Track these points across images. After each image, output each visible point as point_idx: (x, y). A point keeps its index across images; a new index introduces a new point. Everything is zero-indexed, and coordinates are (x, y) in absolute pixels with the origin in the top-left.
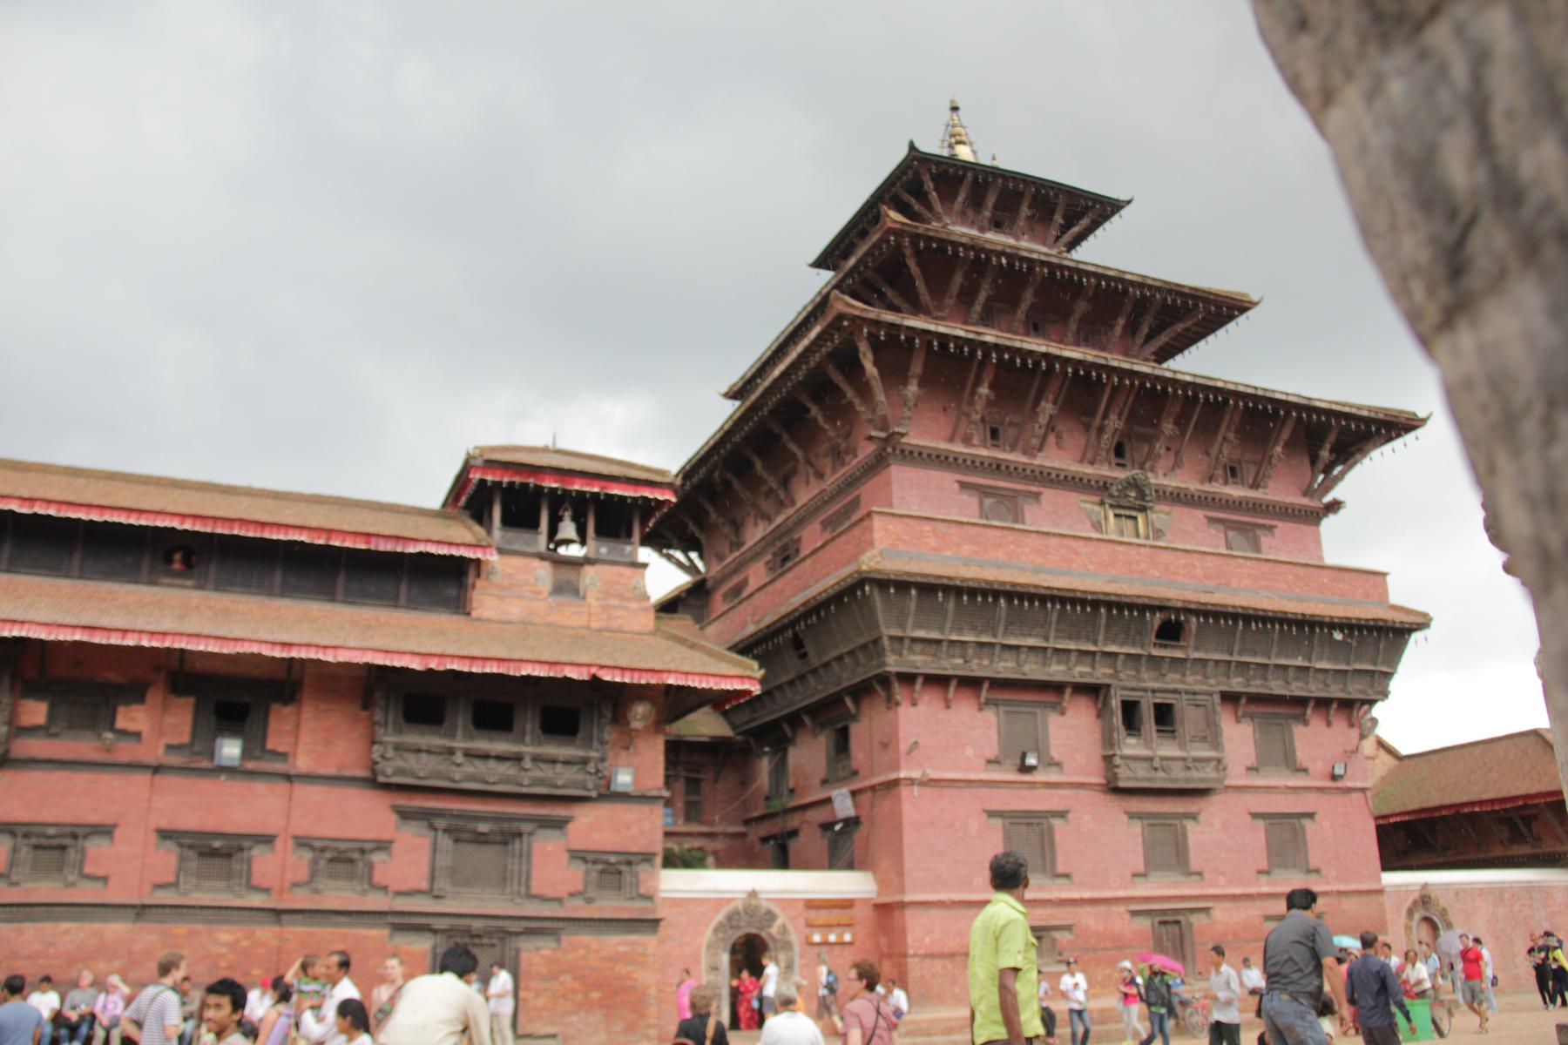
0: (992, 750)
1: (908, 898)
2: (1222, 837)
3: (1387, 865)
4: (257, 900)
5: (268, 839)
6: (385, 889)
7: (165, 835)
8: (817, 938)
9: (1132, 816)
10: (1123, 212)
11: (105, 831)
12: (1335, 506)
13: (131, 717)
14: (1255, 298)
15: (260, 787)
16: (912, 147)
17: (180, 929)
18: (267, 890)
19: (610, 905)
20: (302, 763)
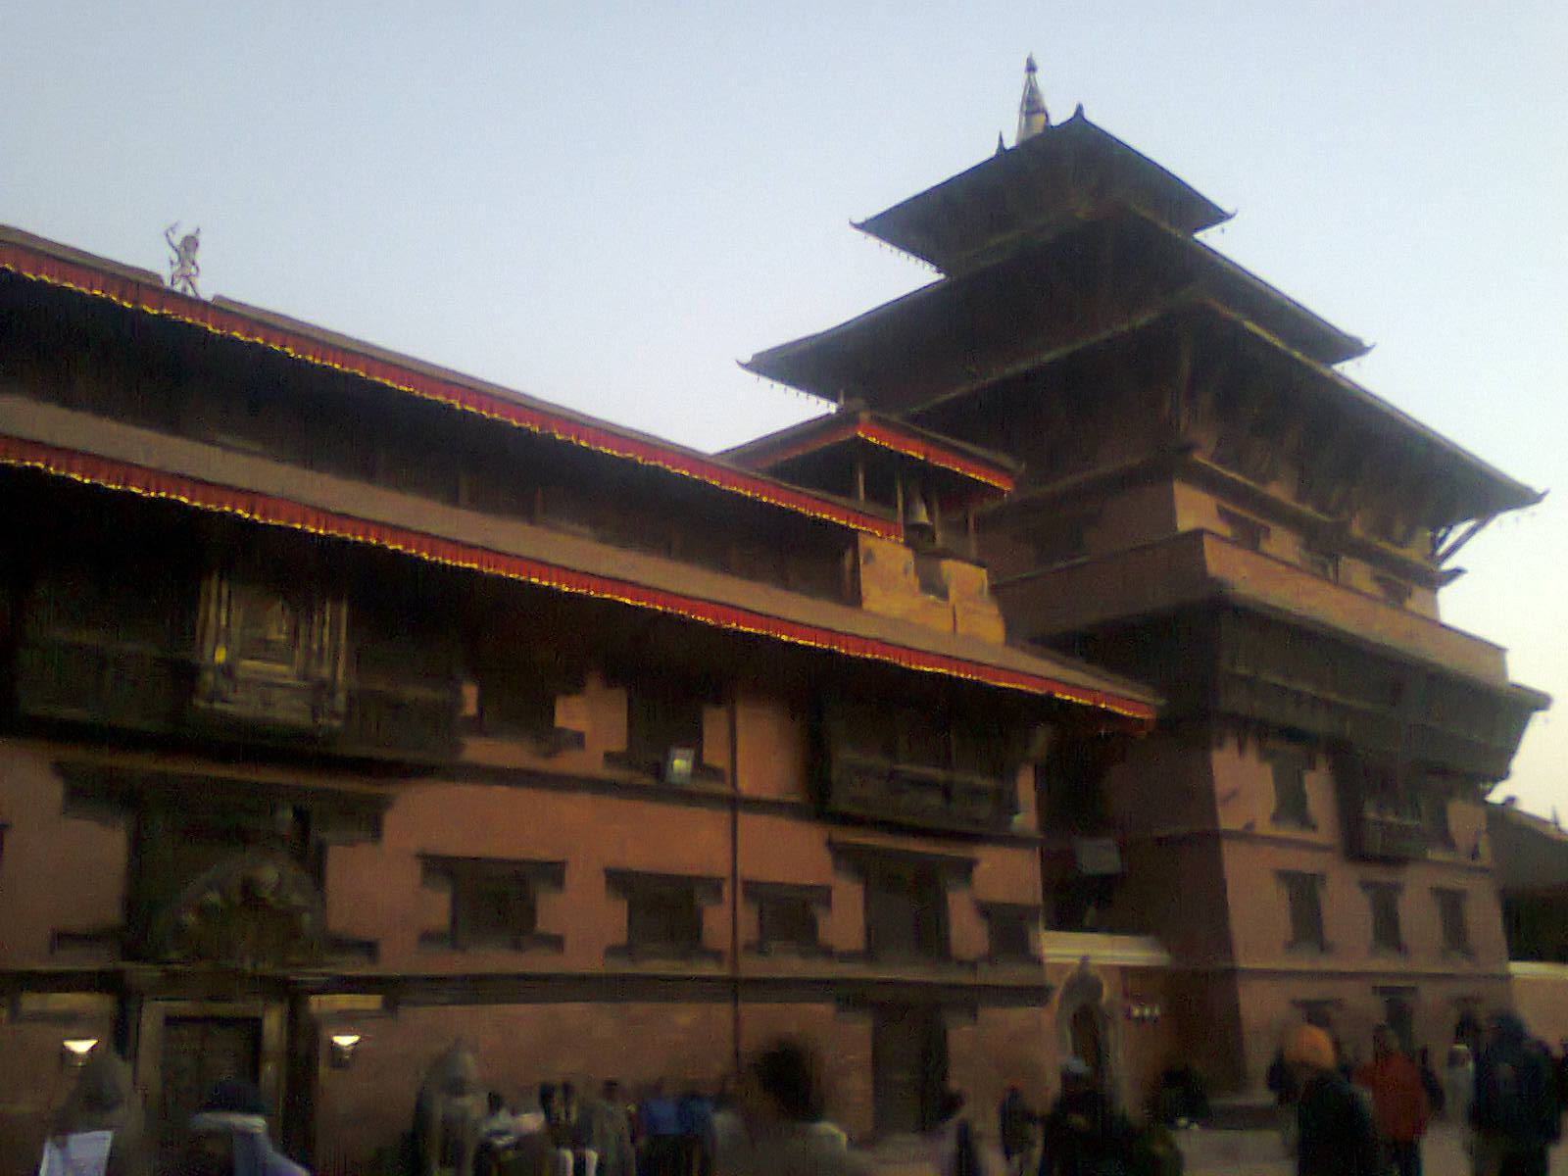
0: (1272, 809)
1: (1243, 965)
2: (1417, 914)
3: (1519, 955)
4: (709, 969)
5: (714, 886)
6: (828, 953)
7: (619, 880)
8: (1136, 1012)
9: (1366, 886)
10: (1226, 225)
11: (553, 873)
12: (1457, 572)
13: (571, 714)
14: (1367, 343)
15: (702, 814)
16: (1079, 110)
17: (638, 1008)
18: (717, 956)
19: (1012, 974)
20: (746, 785)
